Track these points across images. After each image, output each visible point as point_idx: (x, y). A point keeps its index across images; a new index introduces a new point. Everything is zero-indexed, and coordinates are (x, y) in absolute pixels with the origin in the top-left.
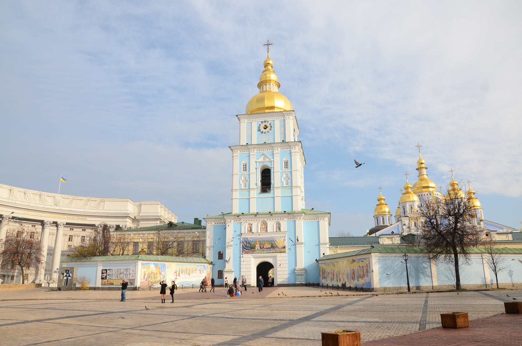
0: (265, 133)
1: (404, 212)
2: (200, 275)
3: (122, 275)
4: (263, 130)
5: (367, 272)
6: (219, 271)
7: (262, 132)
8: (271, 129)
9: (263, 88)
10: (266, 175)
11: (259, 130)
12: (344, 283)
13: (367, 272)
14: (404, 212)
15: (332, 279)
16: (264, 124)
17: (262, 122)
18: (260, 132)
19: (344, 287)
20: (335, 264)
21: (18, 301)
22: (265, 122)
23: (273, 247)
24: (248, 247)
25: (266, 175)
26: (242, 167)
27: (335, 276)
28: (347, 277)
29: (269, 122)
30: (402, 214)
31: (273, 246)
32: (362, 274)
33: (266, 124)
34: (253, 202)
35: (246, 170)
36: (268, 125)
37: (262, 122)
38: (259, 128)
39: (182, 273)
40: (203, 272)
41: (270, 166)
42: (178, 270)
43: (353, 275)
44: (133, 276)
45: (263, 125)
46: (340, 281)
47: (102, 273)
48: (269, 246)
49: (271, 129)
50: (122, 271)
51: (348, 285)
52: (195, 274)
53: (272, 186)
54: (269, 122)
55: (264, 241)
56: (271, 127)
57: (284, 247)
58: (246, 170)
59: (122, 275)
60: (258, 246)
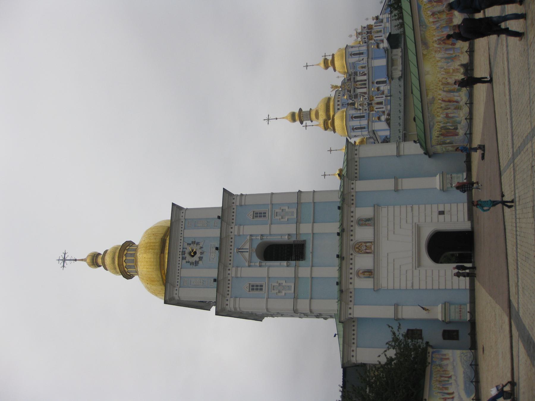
0: (202, 253)
1: (362, 128)
2: (451, 360)
4: (196, 258)
6: (444, 338)
7: (201, 258)
8: (198, 244)
9: (130, 267)
10: (273, 252)
11: (196, 263)
12: (462, 70)
14: (362, 128)
15: (458, 108)
16: (187, 255)
17: (184, 258)
18: (200, 262)
20: (430, 96)
22: (183, 253)
25: (273, 252)
26: (255, 292)
27: (451, 96)
28: (452, 59)
29: (186, 245)
30: (365, 133)
33: (187, 251)
35: (262, 286)
36: (189, 249)
37: (184, 258)
38: (192, 263)
39: (447, 389)
40: (445, 355)
41: (259, 241)
42: (440, 395)
45: (189, 258)
52: (450, 368)
53: (294, 239)
54: (186, 245)
56: (194, 243)
58: (262, 286)
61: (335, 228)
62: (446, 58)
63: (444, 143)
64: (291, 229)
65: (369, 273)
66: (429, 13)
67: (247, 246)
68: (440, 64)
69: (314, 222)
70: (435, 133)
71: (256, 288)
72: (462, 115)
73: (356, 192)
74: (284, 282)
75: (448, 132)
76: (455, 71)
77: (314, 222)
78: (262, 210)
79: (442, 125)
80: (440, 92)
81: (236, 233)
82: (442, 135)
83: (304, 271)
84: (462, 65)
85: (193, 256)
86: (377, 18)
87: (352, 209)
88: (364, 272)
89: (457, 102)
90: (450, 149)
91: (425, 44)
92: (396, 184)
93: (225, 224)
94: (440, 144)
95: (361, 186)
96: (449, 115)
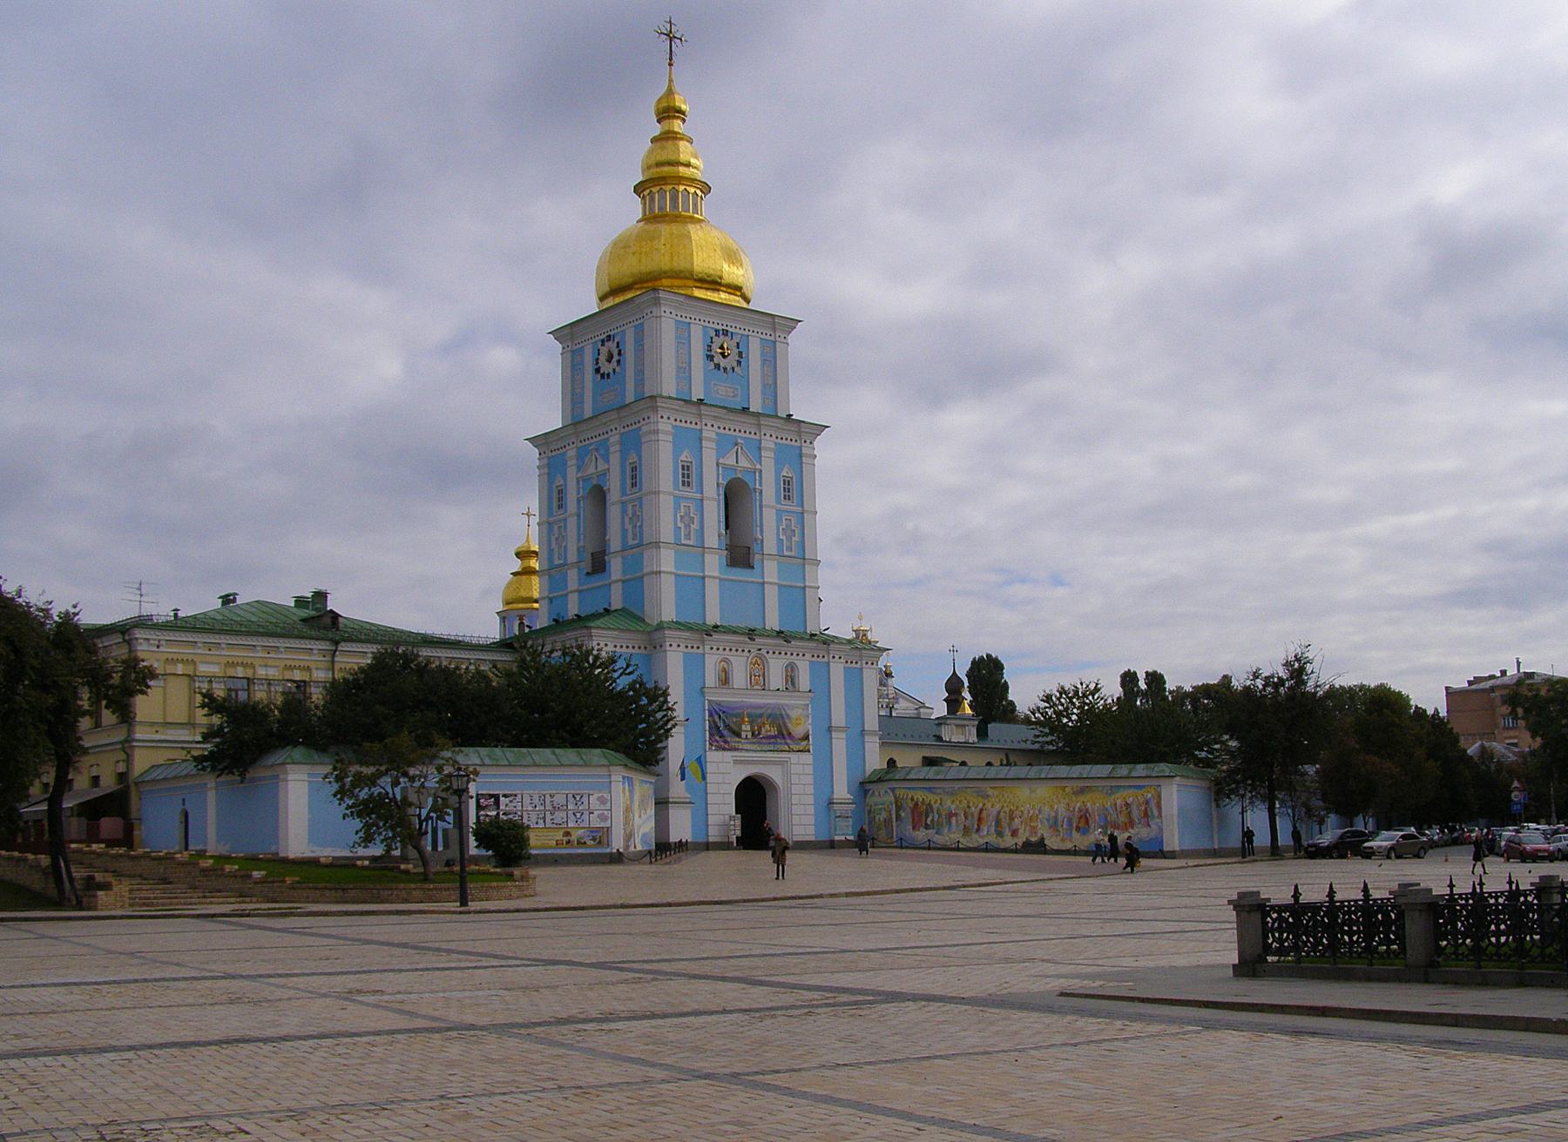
3: (564, 814)
5: (1146, 815)
7: (717, 366)
8: (739, 363)
11: (710, 358)
13: (1146, 815)
19: (1038, 847)
20: (990, 792)
21: (540, 906)
23: (777, 732)
24: (725, 728)
28: (1054, 825)
31: (777, 732)
32: (1122, 819)
34: (712, 590)
43: (1083, 821)
44: (603, 818)
46: (1014, 833)
47: (479, 807)
48: (774, 732)
49: (739, 363)
50: (560, 799)
51: (1052, 843)
53: (756, 548)
55: (761, 716)
56: (740, 354)
57: (806, 738)
59: (559, 816)
60: (746, 727)
61: (773, 623)
62: (1056, 818)
63: (898, 808)
64: (770, 546)
66: (1130, 800)
67: (744, 463)
68: (1047, 809)
69: (780, 586)
70: (919, 796)
71: (687, 475)
72: (952, 835)
73: (828, 663)
74: (695, 526)
75: (920, 815)
76: (1034, 830)
77: (780, 586)
78: (795, 494)
79: (935, 807)
80: (998, 807)
81: (764, 444)
83: (714, 564)
84: (1042, 839)
86: (889, 675)
87: (808, 656)
88: (724, 670)
89: (978, 830)
90: (884, 815)
91: (1082, 791)
92: (839, 729)
93: (778, 423)
95: (837, 670)
96: (954, 820)
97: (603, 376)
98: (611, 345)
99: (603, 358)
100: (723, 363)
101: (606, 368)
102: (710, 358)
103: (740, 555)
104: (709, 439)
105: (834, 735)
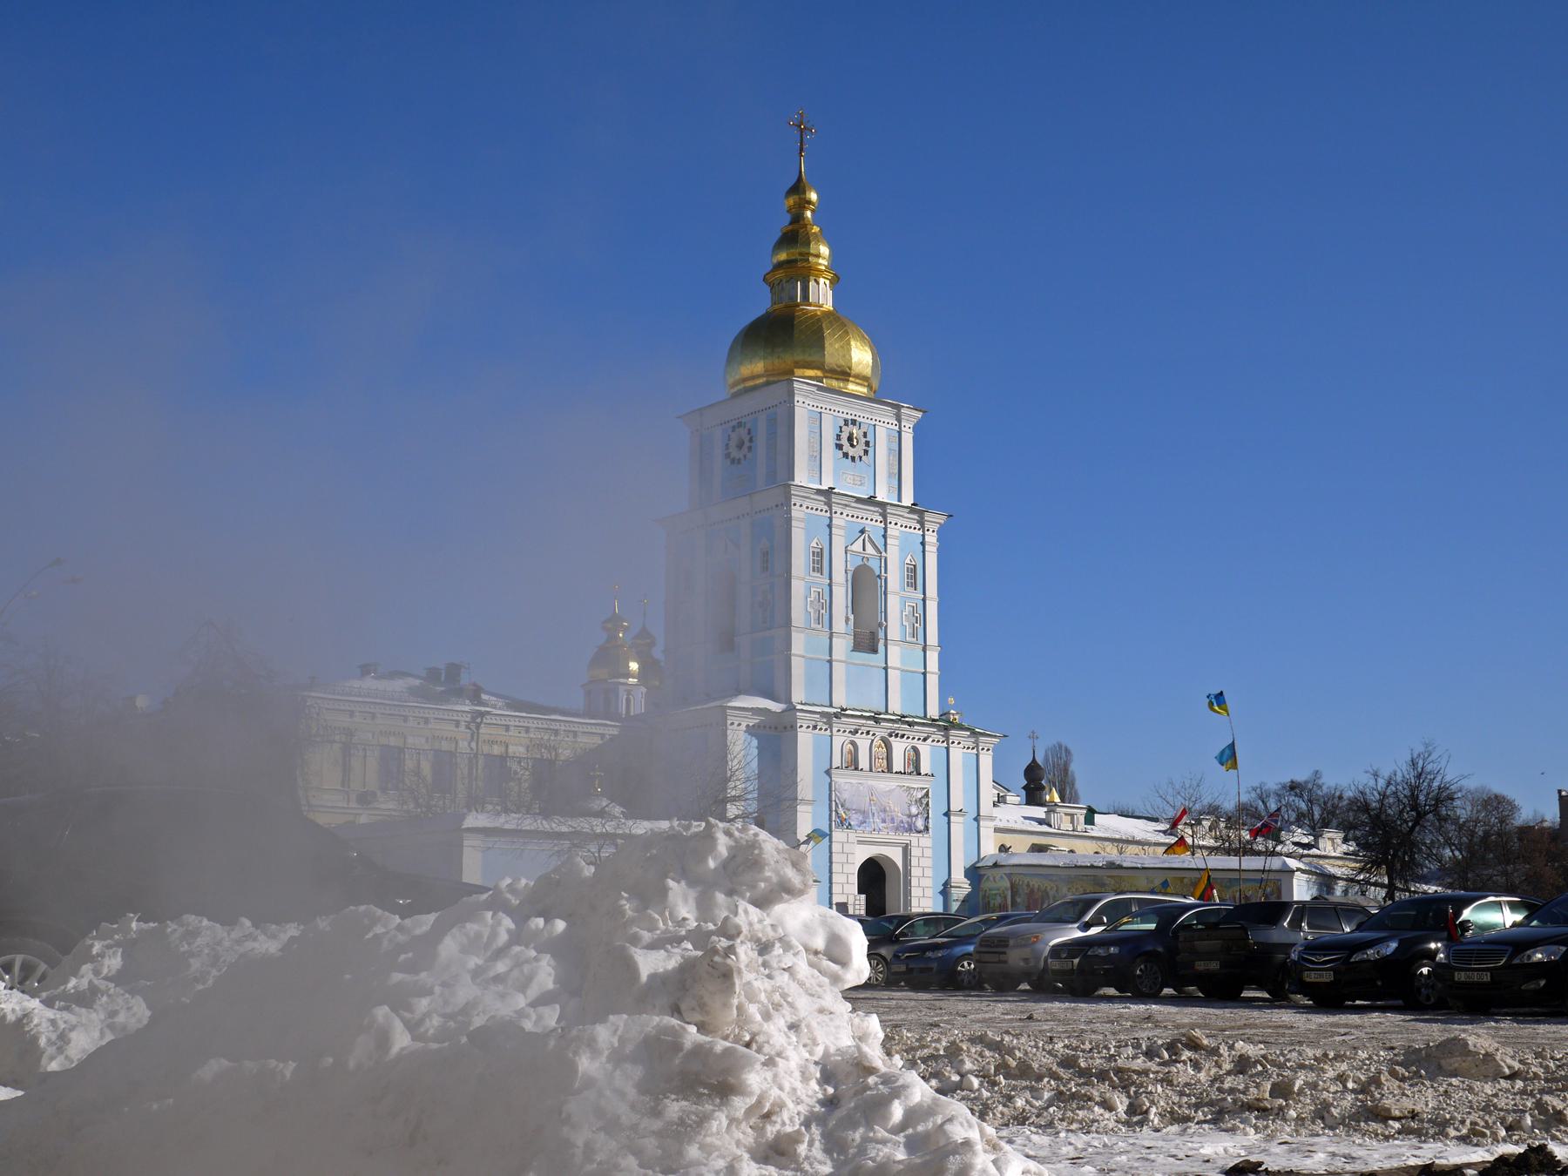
0: (853, 459)
4: (847, 447)
7: (846, 455)
8: (866, 452)
11: (839, 447)
17: (846, 422)
20: (1108, 881)
37: (846, 422)
49: (866, 452)
56: (867, 443)
61: (896, 706)
65: (854, 764)
70: (1035, 883)
71: (820, 560)
79: (1051, 893)
82: (1032, 891)
83: (842, 646)
85: (850, 439)
94: (1013, 886)
97: (733, 461)
98: (743, 432)
99: (733, 444)
100: (851, 452)
101: (735, 454)
102: (839, 447)
103: (868, 641)
104: (839, 527)
105: (953, 818)
